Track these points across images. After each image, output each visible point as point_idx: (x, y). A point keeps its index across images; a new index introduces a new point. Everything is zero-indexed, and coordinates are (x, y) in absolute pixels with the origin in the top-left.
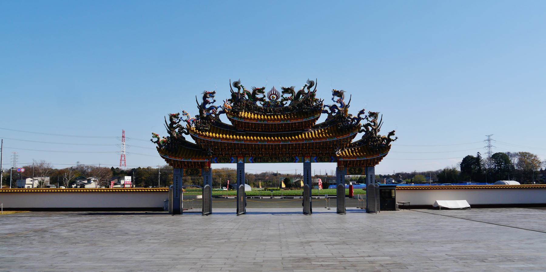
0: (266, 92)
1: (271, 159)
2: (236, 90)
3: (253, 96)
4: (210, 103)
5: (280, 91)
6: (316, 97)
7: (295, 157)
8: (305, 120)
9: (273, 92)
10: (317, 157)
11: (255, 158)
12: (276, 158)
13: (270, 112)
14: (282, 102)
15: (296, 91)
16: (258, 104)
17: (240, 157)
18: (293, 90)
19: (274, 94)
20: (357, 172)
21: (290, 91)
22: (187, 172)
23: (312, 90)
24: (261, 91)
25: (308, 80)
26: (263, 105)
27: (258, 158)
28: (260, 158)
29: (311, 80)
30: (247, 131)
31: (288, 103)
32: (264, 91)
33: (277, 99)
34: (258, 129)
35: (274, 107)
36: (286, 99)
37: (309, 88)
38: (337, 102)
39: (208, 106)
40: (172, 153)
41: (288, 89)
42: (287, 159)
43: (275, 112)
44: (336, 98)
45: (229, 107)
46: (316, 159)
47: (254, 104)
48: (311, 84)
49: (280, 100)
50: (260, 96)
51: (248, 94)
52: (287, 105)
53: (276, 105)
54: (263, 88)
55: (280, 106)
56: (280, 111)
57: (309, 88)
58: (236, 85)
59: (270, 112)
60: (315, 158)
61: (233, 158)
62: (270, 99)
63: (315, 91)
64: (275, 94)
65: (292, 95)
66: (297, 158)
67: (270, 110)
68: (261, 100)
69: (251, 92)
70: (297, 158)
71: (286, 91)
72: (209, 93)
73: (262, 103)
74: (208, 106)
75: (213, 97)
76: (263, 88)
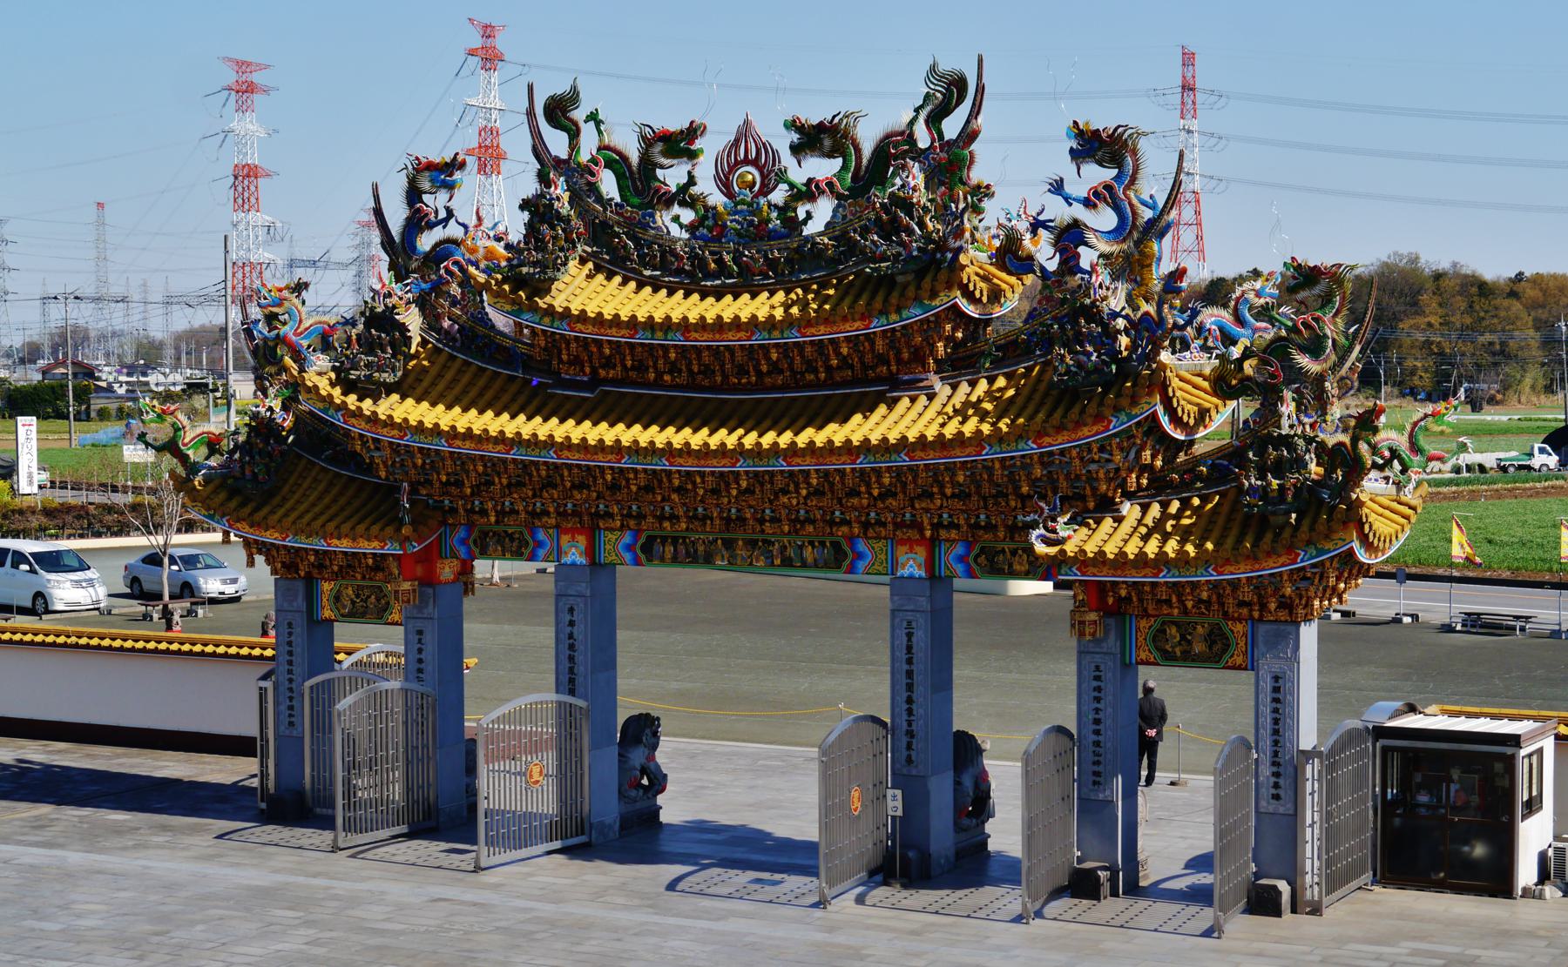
0: (711, 147)
1: (729, 544)
2: (557, 143)
3: (639, 180)
4: (431, 226)
5: (782, 141)
6: (977, 175)
7: (851, 539)
8: (878, 325)
9: (746, 152)
10: (969, 546)
11: (651, 539)
12: (752, 544)
13: (723, 270)
14: (785, 210)
15: (868, 137)
16: (674, 223)
17: (573, 532)
18: (846, 135)
19: (746, 162)
20: (1198, 647)
21: (827, 143)
22: (337, 598)
23: (952, 126)
24: (680, 144)
25: (933, 69)
26: (691, 228)
27: (664, 540)
28: (675, 541)
29: (945, 66)
30: (606, 381)
31: (819, 215)
32: (698, 144)
33: (766, 190)
35: (748, 245)
36: (809, 192)
37: (934, 120)
38: (1087, 203)
39: (426, 242)
40: (242, 505)
41: (821, 127)
42: (808, 553)
43: (745, 271)
44: (1097, 174)
45: (490, 255)
46: (962, 559)
47: (646, 227)
48: (950, 92)
49: (779, 195)
50: (672, 175)
51: (617, 162)
52: (811, 229)
53: (757, 232)
54: (693, 132)
55: (774, 235)
56: (772, 264)
57: (934, 120)
58: (559, 111)
59: (723, 270)
60: (959, 549)
61: (541, 536)
62: (729, 194)
63: (969, 135)
64: (755, 163)
65: (844, 167)
66: (861, 546)
67: (720, 262)
68: (684, 196)
69: (634, 158)
70: (861, 546)
71: (811, 138)
72: (430, 167)
73: (688, 216)
74: (426, 242)
75: (450, 187)
76: (693, 132)
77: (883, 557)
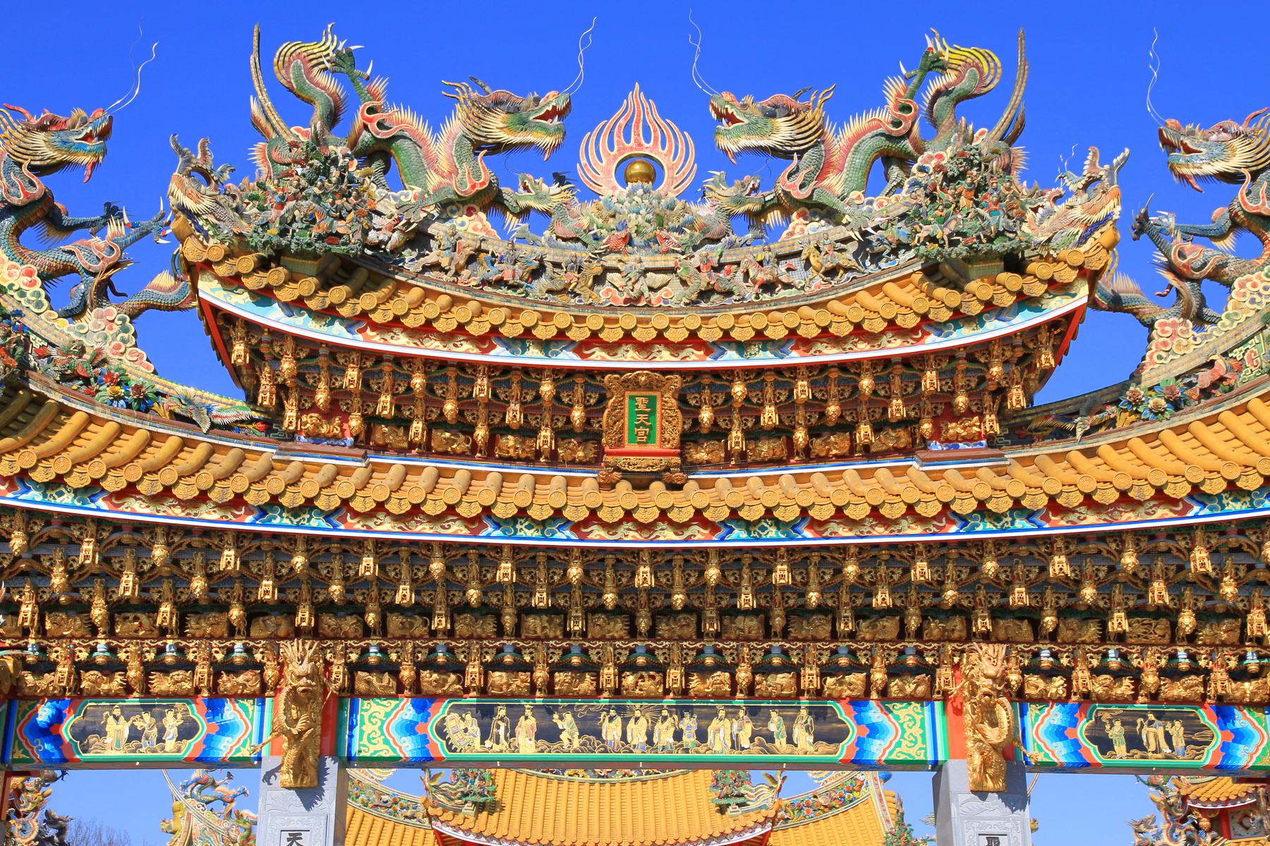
34: (499, 430)
77: (916, 730)
